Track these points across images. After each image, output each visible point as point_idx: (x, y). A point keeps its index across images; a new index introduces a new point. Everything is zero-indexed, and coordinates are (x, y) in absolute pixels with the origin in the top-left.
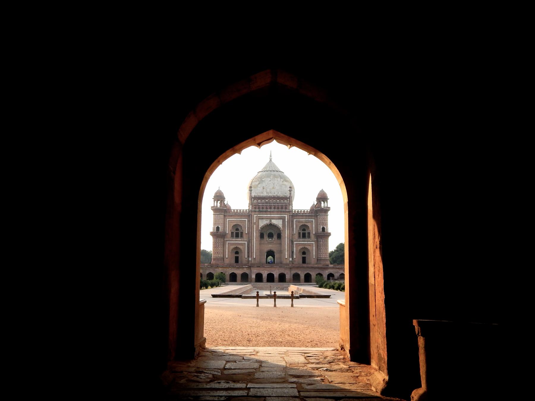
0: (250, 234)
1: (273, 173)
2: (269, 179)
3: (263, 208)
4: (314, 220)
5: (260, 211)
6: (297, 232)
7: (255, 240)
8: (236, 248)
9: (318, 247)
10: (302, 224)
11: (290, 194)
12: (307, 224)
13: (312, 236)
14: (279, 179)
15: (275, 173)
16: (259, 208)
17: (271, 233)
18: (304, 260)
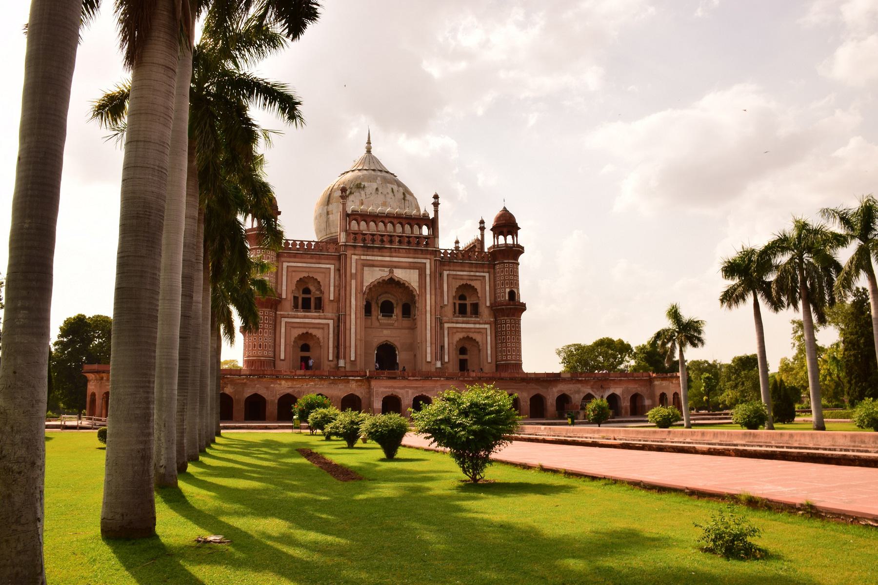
0: (341, 300)
1: (379, 173)
2: (375, 186)
3: (373, 241)
4: (487, 275)
5: (366, 248)
6: (451, 301)
7: (353, 316)
8: (306, 336)
9: (498, 334)
10: (462, 282)
11: (436, 212)
12: (473, 283)
13: (485, 312)
14: (395, 187)
15: (384, 174)
16: (364, 240)
17: (391, 300)
18: (463, 365)
